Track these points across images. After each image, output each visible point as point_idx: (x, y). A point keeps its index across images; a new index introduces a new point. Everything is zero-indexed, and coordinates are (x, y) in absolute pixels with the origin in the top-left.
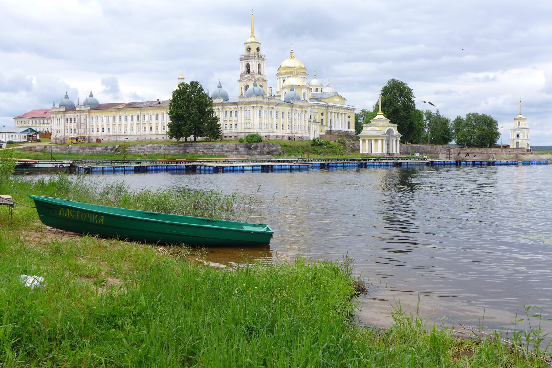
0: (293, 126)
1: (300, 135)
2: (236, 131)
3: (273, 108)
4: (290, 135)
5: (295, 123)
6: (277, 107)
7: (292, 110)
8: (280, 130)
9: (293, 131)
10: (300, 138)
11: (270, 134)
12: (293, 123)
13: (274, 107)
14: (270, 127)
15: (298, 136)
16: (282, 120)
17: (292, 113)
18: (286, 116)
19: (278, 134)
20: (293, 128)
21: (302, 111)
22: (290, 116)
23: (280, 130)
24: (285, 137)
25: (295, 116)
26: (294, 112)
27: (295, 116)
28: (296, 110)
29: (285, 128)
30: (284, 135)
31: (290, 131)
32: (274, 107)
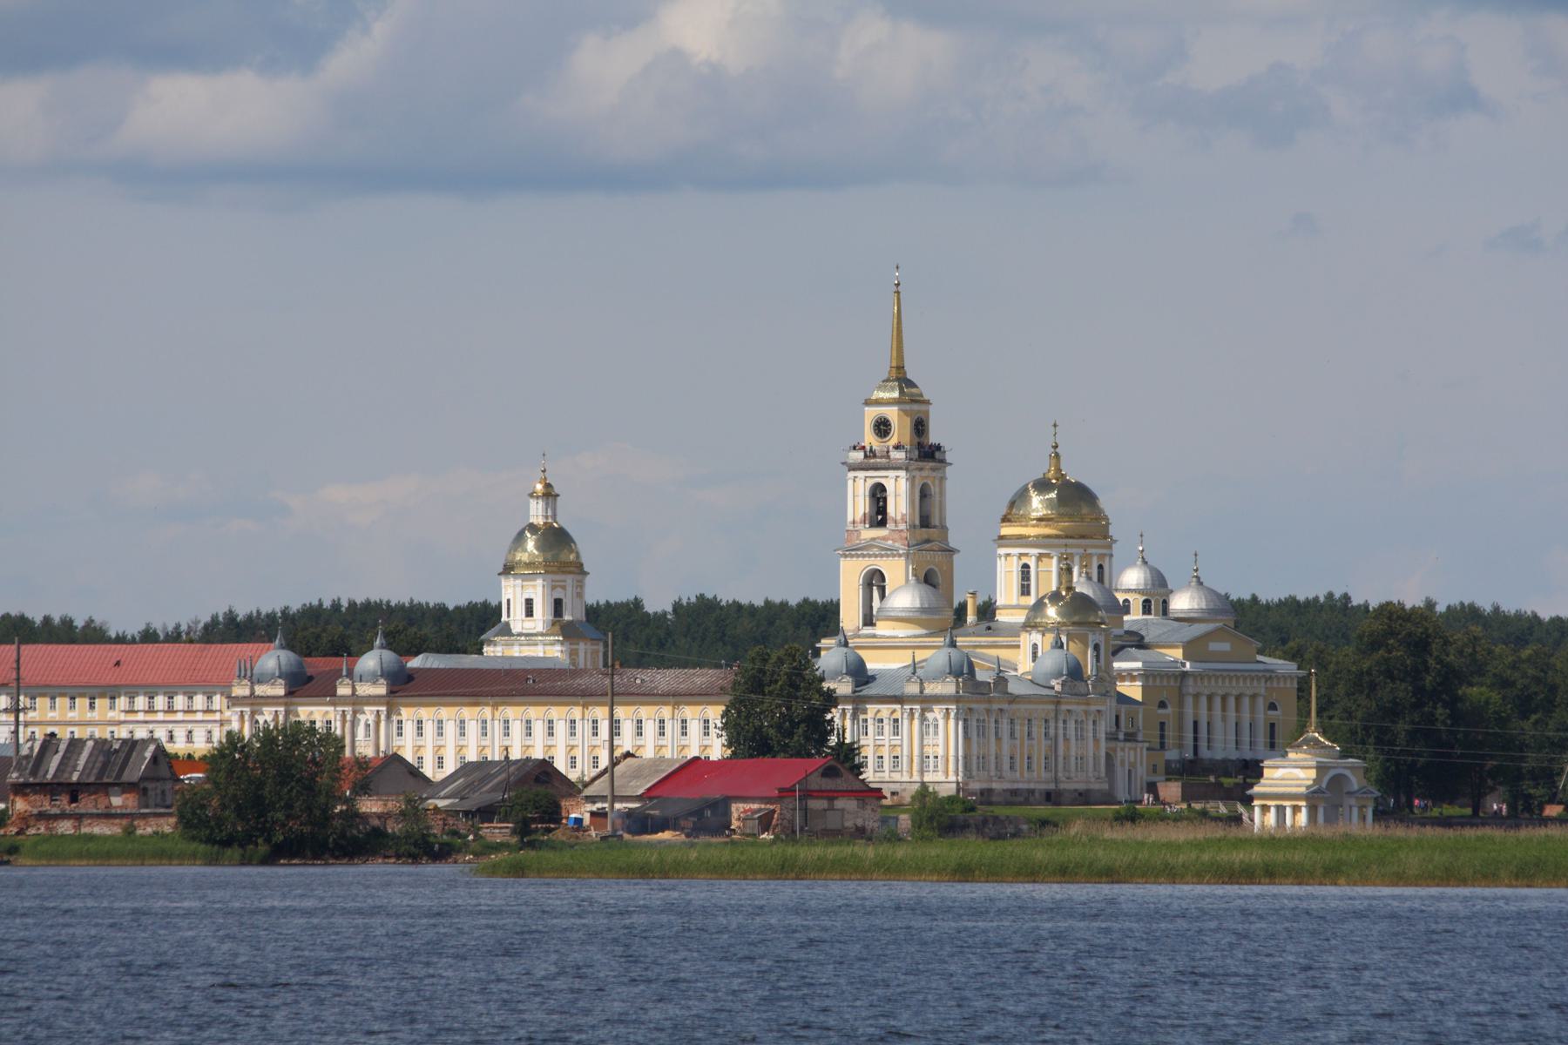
0: (1061, 759)
1: (1081, 787)
2: (896, 777)
3: (1001, 710)
4: (1052, 786)
5: (1067, 748)
6: (1015, 707)
7: (1057, 712)
8: (1022, 774)
9: (1060, 774)
10: (1080, 794)
11: (995, 786)
12: (1061, 752)
13: (1005, 706)
14: (993, 766)
15: (1076, 790)
16: (1026, 742)
17: (1056, 722)
18: (1039, 730)
19: (1016, 786)
20: (1061, 766)
21: (1086, 713)
22: (1052, 732)
23: (1022, 774)
24: (1037, 795)
25: (1065, 729)
26: (1061, 718)
27: (1065, 729)
28: (1069, 711)
29: (1035, 766)
30: (1032, 786)
31: (1050, 775)
32: (1005, 706)
